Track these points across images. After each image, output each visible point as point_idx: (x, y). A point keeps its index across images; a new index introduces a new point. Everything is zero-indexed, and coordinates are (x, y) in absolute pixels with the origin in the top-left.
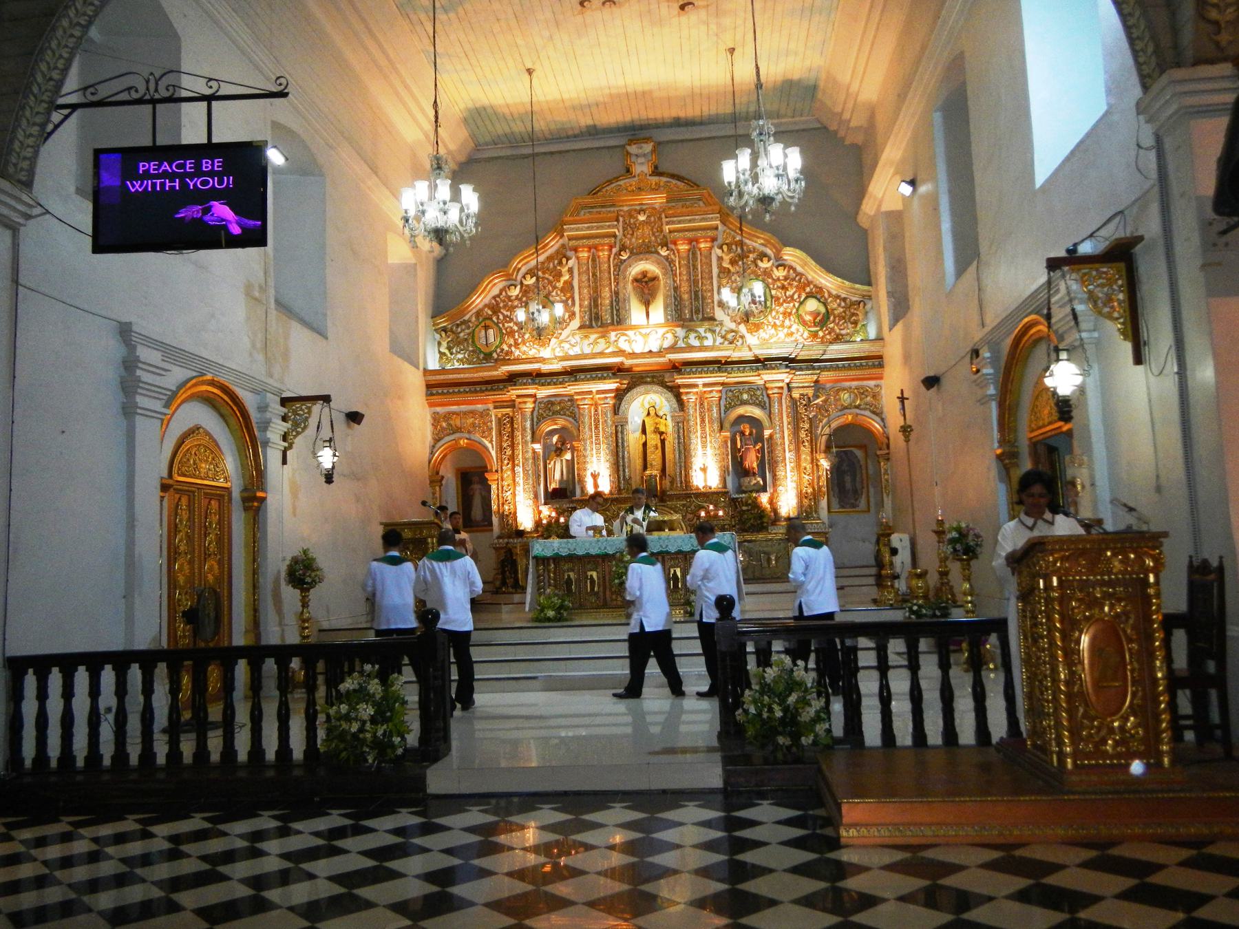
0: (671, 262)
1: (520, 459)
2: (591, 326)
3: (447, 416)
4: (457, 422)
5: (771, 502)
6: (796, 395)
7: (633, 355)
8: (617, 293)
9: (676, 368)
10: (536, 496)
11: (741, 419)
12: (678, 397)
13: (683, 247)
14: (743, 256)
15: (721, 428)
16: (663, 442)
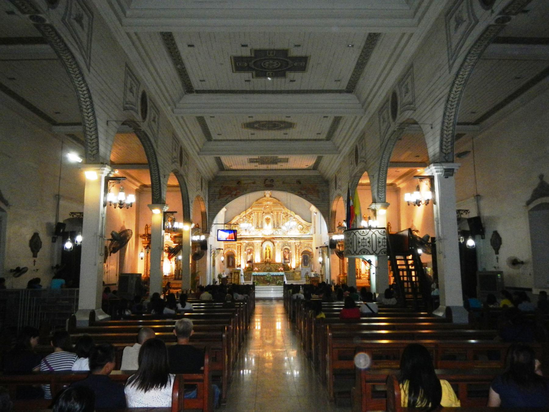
0: (273, 216)
1: (242, 255)
2: (256, 228)
3: (227, 245)
4: (229, 246)
5: (290, 265)
6: (296, 244)
7: (266, 235)
8: (262, 222)
9: (273, 238)
10: (245, 262)
11: (286, 249)
12: (273, 244)
13: (276, 213)
14: (287, 216)
15: (282, 250)
16: (270, 252)
